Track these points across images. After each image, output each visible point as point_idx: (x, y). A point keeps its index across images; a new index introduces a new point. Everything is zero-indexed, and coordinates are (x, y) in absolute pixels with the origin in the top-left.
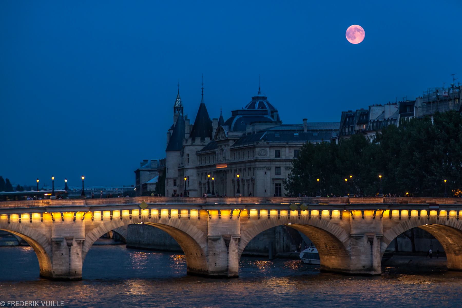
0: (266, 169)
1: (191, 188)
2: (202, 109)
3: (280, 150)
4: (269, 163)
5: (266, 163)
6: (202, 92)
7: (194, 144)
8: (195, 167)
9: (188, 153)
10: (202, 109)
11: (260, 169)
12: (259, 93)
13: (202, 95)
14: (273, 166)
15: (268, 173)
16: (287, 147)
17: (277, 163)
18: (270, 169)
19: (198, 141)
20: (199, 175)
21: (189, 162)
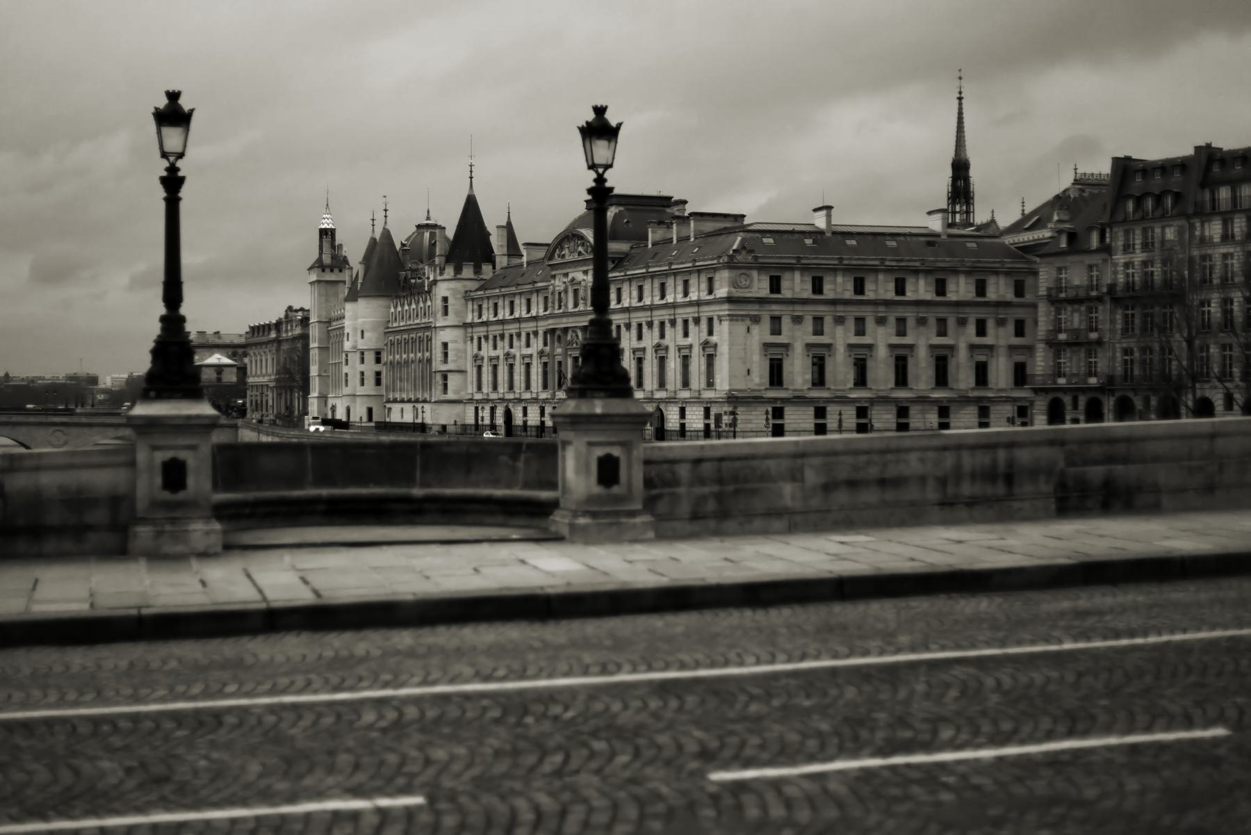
0: (751, 320)
1: (450, 366)
2: (471, 208)
3: (780, 276)
4: (757, 307)
5: (750, 307)
6: (471, 172)
7: (458, 276)
8: (461, 324)
9: (445, 295)
10: (471, 208)
11: (737, 320)
12: (428, 218)
13: (471, 178)
14: (765, 314)
15: (755, 330)
16: (798, 269)
17: (774, 307)
18: (760, 320)
19: (468, 272)
20: (472, 339)
21: (446, 313)
